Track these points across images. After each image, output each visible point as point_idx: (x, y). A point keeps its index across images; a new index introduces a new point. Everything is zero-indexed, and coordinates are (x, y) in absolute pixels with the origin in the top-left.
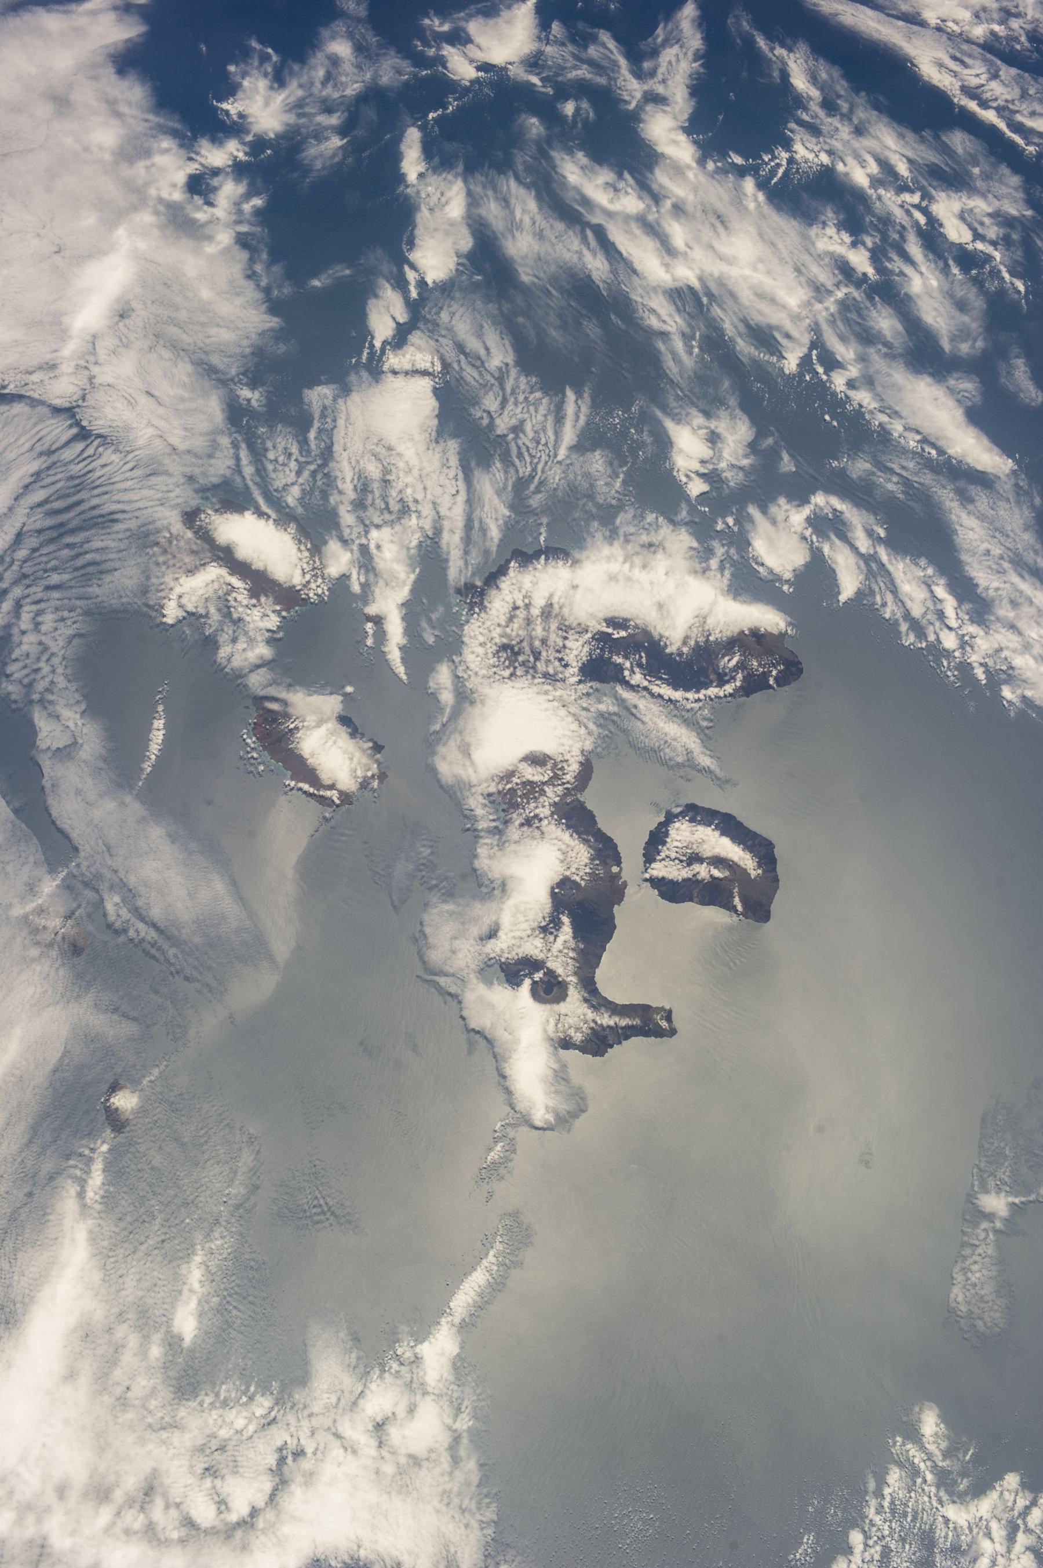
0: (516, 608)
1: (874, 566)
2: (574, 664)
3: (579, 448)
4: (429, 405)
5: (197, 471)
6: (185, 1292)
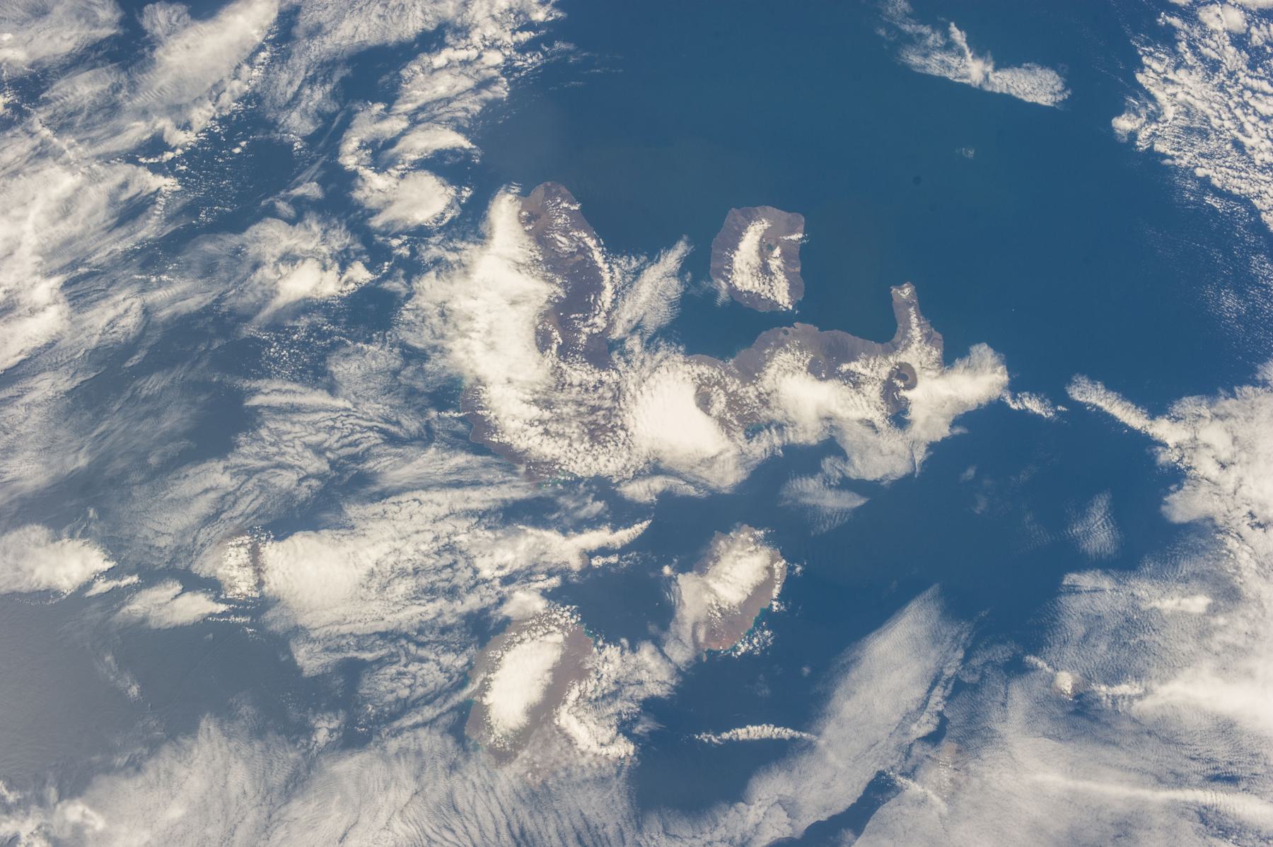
0: (546, 432)
1: (420, 116)
2: (597, 376)
3: (332, 389)
4: (300, 541)
5: (441, 763)
6: (1181, 608)
